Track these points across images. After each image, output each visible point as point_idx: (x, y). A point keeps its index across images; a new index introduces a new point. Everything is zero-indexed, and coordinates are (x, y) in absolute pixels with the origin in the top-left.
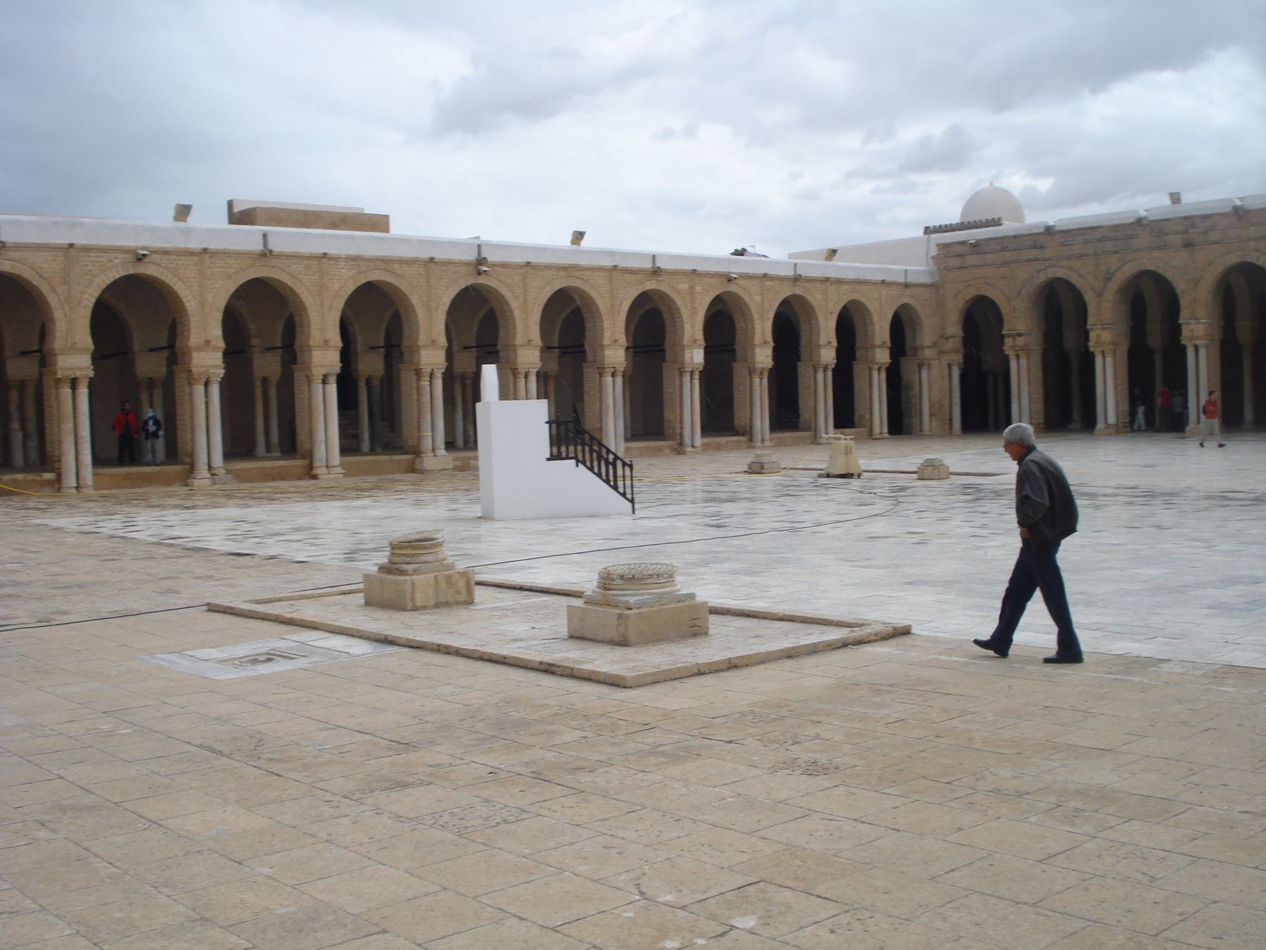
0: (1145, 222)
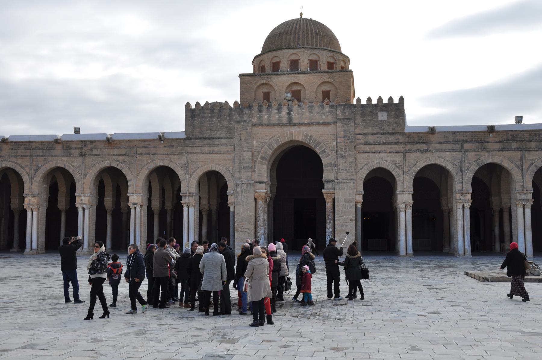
0: (59, 141)
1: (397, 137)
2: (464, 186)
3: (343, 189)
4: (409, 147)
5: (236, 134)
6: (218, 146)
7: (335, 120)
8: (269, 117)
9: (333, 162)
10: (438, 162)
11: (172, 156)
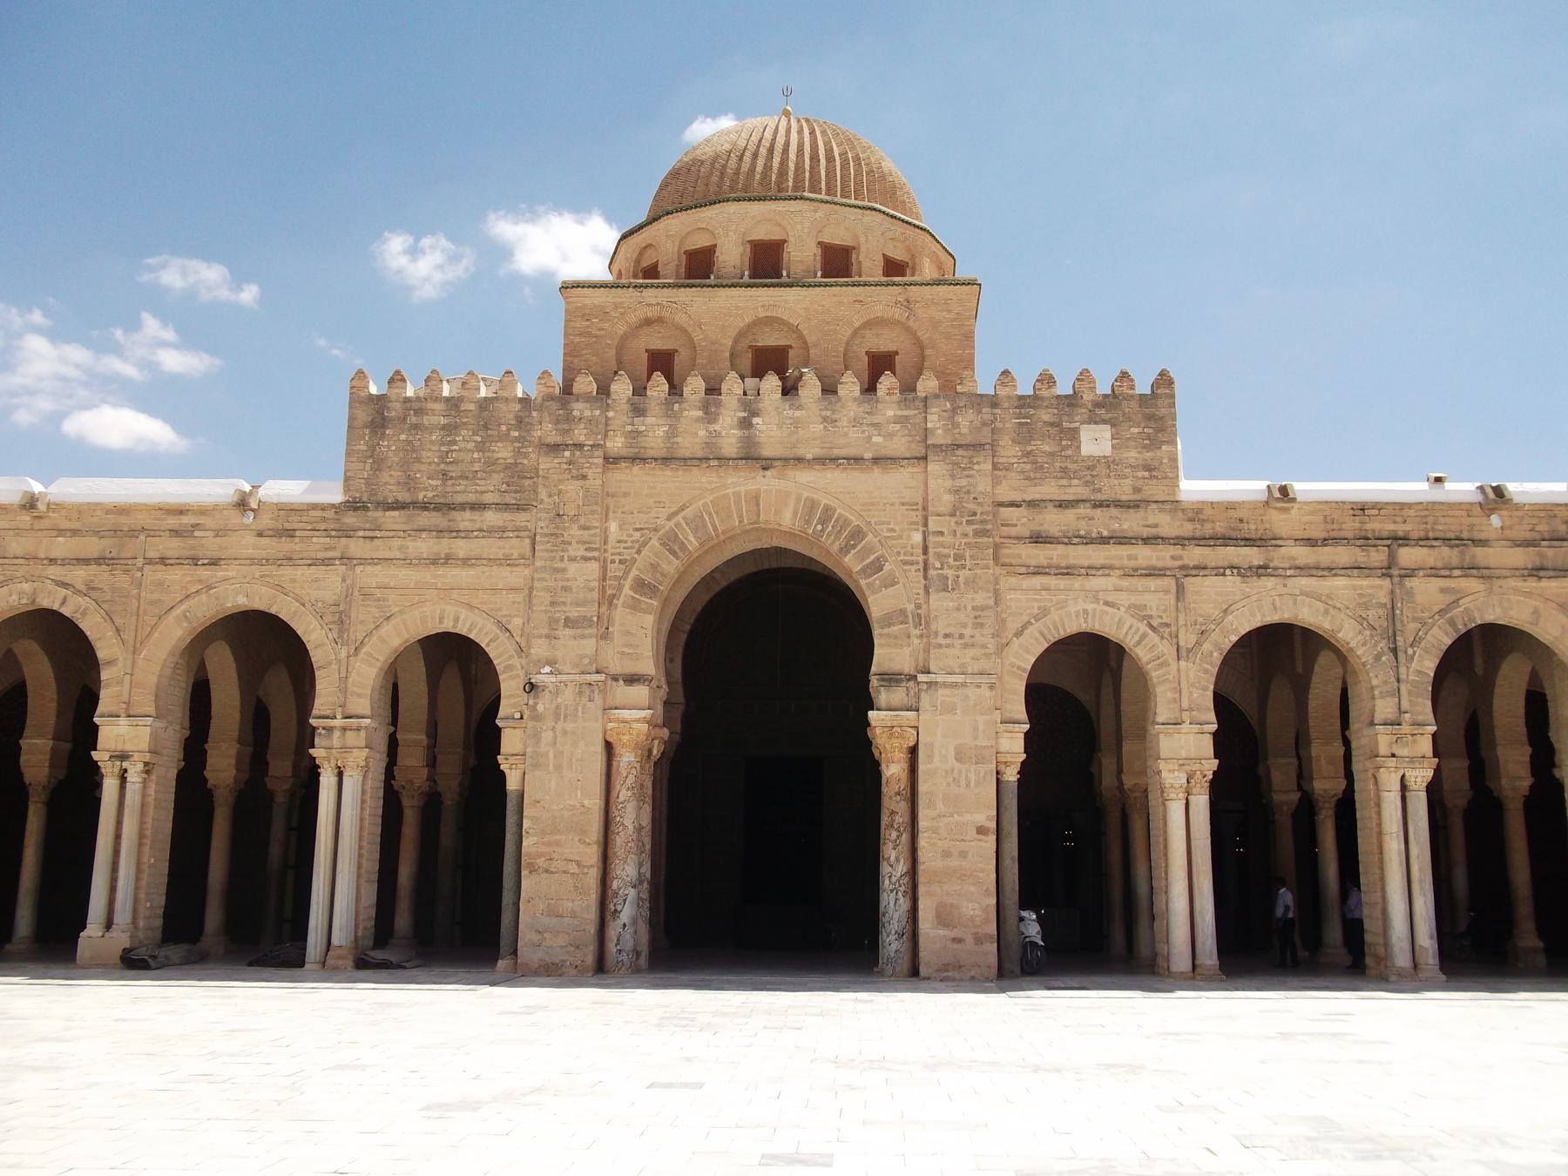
1: (1151, 521)
2: (1405, 705)
3: (951, 709)
4: (1194, 555)
5: (543, 494)
6: (467, 534)
7: (920, 451)
8: (673, 432)
9: (910, 607)
10: (1307, 615)
11: (288, 572)
